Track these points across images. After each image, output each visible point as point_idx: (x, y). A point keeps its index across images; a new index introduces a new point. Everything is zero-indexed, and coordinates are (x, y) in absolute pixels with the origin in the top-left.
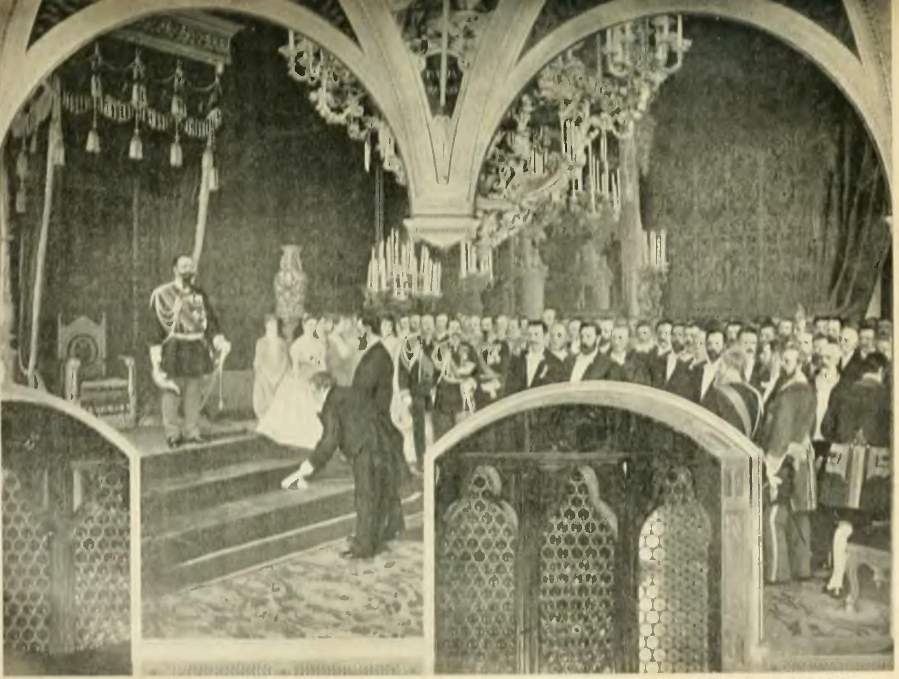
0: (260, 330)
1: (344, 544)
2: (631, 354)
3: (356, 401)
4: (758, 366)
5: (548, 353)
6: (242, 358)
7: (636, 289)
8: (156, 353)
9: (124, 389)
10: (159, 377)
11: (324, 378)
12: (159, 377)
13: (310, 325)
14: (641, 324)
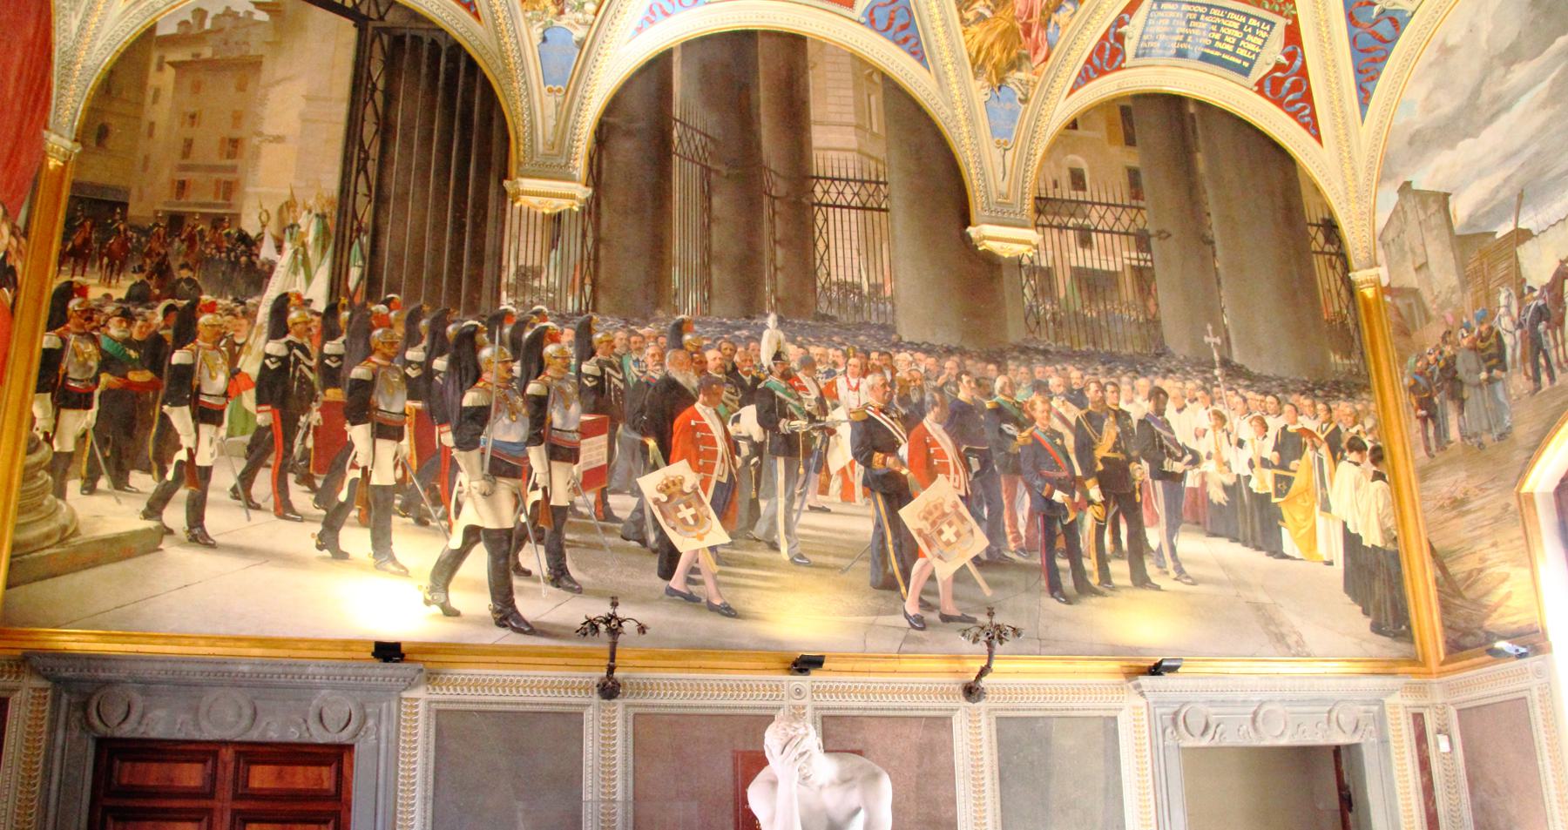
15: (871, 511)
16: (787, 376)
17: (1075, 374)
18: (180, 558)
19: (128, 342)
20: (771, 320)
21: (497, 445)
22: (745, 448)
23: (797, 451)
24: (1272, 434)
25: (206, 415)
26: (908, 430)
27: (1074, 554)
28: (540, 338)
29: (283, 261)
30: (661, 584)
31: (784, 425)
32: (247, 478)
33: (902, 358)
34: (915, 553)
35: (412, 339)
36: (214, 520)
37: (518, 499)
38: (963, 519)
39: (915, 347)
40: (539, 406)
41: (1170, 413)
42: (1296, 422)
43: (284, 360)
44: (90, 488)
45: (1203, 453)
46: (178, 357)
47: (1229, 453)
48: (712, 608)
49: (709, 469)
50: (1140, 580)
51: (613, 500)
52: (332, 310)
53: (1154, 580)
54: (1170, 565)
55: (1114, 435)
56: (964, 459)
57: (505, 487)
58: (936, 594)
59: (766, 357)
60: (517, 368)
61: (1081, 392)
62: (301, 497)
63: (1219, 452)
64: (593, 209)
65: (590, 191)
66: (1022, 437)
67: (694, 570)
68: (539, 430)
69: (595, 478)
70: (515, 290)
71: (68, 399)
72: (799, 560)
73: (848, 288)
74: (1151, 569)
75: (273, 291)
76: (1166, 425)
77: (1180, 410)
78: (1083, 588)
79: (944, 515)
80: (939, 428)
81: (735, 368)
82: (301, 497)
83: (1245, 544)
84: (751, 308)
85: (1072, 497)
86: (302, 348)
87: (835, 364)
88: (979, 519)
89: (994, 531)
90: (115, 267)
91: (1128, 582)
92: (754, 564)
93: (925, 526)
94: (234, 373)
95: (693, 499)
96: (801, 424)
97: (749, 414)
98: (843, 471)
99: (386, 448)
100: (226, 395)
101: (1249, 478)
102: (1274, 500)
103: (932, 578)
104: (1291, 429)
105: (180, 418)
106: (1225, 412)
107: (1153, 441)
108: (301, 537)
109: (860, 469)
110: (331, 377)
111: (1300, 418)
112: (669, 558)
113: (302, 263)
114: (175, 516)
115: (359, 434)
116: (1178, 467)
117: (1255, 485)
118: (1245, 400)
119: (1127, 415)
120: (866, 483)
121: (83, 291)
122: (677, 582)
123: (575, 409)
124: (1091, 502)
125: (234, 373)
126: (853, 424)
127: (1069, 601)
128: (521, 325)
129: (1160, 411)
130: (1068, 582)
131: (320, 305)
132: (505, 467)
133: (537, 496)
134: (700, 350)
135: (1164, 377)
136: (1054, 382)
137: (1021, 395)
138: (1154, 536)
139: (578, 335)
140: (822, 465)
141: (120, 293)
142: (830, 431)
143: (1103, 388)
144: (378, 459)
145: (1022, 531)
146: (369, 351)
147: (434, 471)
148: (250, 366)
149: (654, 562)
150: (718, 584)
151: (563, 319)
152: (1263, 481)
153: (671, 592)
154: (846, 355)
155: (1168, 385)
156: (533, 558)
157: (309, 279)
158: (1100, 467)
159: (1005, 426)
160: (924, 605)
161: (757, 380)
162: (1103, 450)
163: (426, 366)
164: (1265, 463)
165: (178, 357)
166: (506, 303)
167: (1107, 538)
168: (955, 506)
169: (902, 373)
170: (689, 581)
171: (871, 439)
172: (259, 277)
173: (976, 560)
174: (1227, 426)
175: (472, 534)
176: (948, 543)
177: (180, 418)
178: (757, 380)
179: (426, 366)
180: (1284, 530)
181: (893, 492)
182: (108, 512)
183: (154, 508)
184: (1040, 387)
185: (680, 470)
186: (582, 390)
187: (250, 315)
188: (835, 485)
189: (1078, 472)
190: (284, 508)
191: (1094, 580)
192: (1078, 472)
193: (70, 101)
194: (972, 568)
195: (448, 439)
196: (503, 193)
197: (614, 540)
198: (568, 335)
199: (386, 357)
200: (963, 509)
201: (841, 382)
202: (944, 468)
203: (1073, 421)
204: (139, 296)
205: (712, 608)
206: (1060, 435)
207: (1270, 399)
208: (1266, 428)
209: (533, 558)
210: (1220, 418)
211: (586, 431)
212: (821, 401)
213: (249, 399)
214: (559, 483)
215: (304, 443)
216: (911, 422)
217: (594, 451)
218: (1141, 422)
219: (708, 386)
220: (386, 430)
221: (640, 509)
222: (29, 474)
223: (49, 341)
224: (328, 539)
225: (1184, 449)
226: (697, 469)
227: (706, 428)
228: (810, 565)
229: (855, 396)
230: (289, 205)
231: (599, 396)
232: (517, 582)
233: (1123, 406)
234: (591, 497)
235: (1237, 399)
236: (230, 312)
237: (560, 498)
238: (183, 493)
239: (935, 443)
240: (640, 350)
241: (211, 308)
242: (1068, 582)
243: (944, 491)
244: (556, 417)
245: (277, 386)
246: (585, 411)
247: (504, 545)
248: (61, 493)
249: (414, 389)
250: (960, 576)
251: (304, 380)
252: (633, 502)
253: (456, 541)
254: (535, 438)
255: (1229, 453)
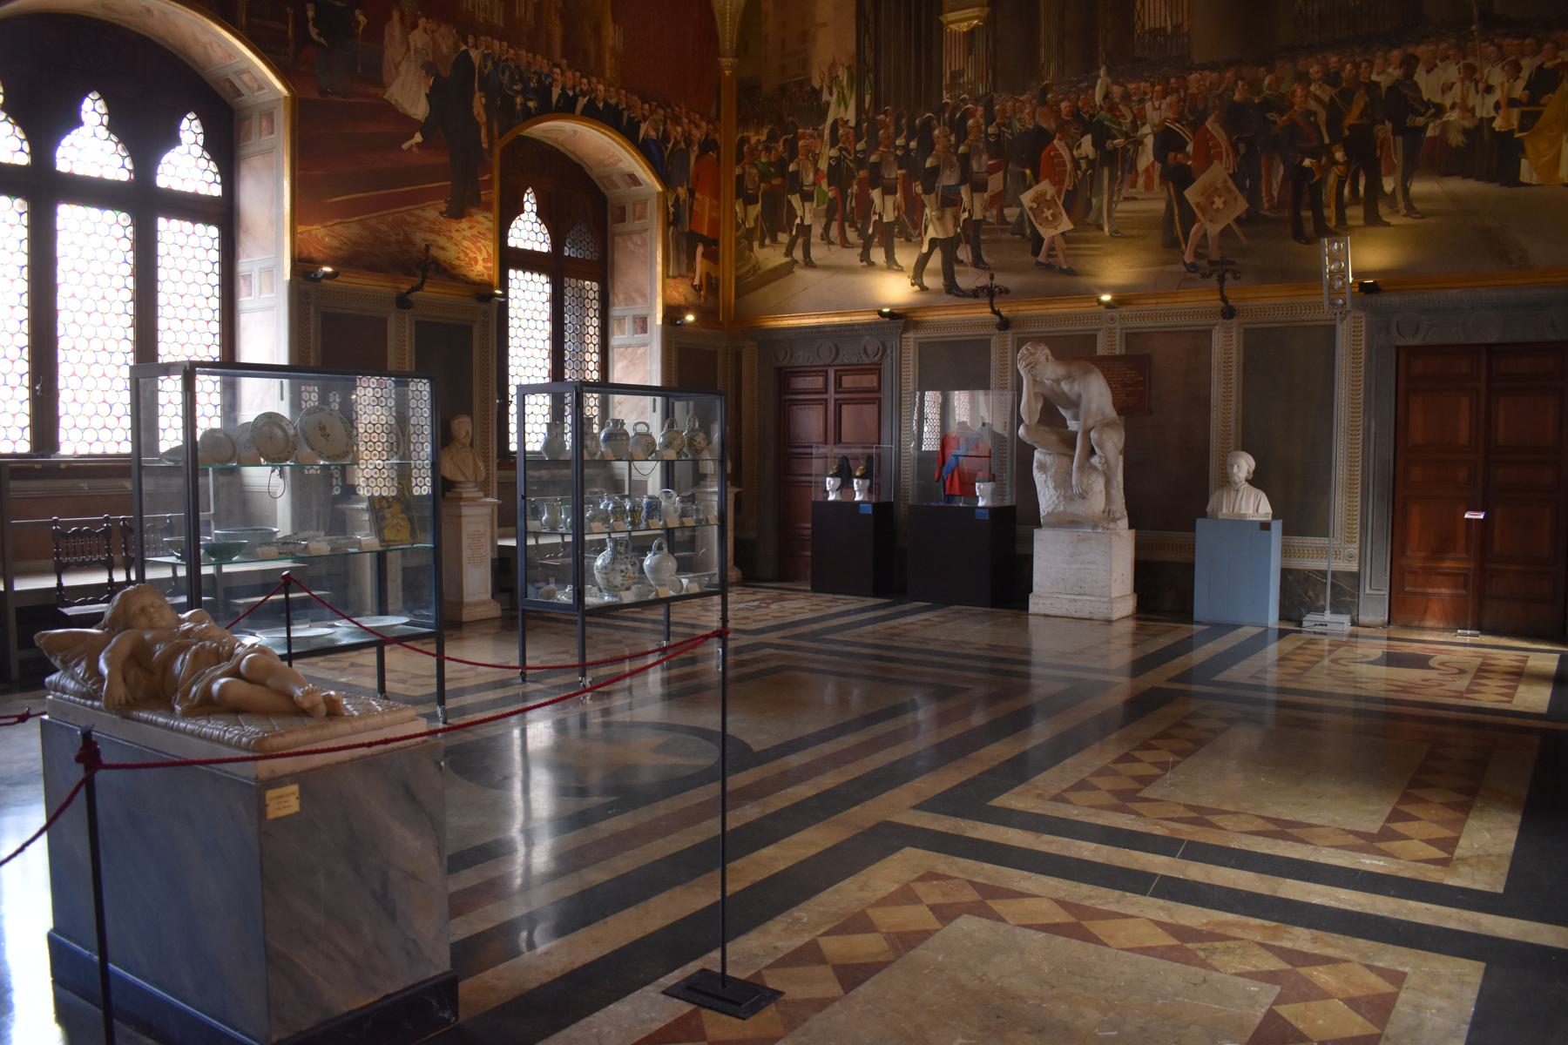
0: (390, 18)
1: (443, 207)
2: (606, 104)
3: (449, 90)
4: (665, 131)
5: (563, 89)
6: (376, 33)
7: (609, 61)
8: (310, 14)
9: (286, 33)
10: (313, 32)
11: (429, 68)
12: (313, 32)
13: (422, 22)
14: (611, 85)
15: (1165, 194)
16: (1112, 108)
17: (1333, 60)
18: (804, 275)
19: (770, 164)
20: (1102, 72)
21: (945, 188)
22: (1083, 165)
23: (1116, 161)
24: (1525, 74)
25: (807, 197)
26: (1194, 133)
27: (1317, 206)
28: (967, 114)
29: (834, 100)
30: (1031, 259)
31: (1109, 145)
32: (827, 228)
33: (1194, 76)
34: (1194, 219)
35: (897, 135)
36: (816, 253)
37: (956, 218)
38: (1229, 191)
39: (1203, 67)
40: (965, 160)
41: (1420, 77)
42: (1556, 57)
43: (838, 159)
44: (762, 245)
45: (1448, 104)
46: (792, 168)
47: (1474, 100)
48: (1063, 271)
49: (1061, 182)
50: (1373, 219)
51: (1007, 211)
52: (859, 123)
53: (1385, 219)
54: (1401, 205)
55: (1362, 104)
56: (1234, 146)
57: (949, 212)
58: (1207, 247)
59: (1098, 99)
60: (953, 138)
61: (1337, 73)
62: (852, 235)
63: (1464, 99)
64: (990, 21)
65: (987, 9)
66: (1281, 120)
67: (1052, 249)
68: (966, 177)
69: (999, 201)
70: (950, 88)
71: (750, 200)
72: (1116, 235)
73: (1155, 32)
74: (1383, 210)
75: (830, 121)
76: (1415, 87)
77: (1428, 72)
78: (1322, 230)
79: (1216, 189)
80: (1217, 126)
81: (1079, 110)
82: (852, 235)
83: (1478, 178)
84: (1089, 69)
85: (1319, 161)
86: (846, 149)
87: (1145, 93)
88: (1241, 188)
89: (1253, 196)
90: (760, 126)
91: (1361, 222)
92: (1087, 241)
93: (1201, 200)
94: (817, 171)
95: (1051, 204)
96: (1119, 141)
97: (1087, 141)
98: (1147, 170)
99: (889, 200)
100: (814, 184)
101: (1493, 119)
102: (1517, 135)
103: (1205, 236)
104: (1548, 65)
105: (795, 200)
106: (1477, 64)
107: (1402, 104)
108: (852, 257)
109: (1158, 166)
110: (861, 163)
111: (1561, 53)
112: (1037, 240)
113: (843, 100)
114: (798, 254)
115: (876, 194)
116: (1420, 121)
117: (1498, 124)
118: (1500, 47)
119: (1377, 84)
120: (1162, 176)
121: (747, 140)
122: (1041, 258)
123: (985, 157)
124: (1336, 163)
125: (817, 171)
126: (1155, 135)
127: (1309, 241)
128: (955, 109)
129: (1409, 75)
130: (1309, 228)
131: (852, 123)
132: (949, 201)
133: (966, 215)
134: (1057, 103)
135: (1418, 44)
136: (1314, 70)
137: (1284, 88)
138: (1388, 185)
139: (985, 110)
140: (1133, 167)
141: (763, 138)
142: (1139, 143)
143: (1357, 66)
144: (886, 207)
145: (1275, 194)
146: (878, 144)
147: (912, 209)
148: (823, 165)
149: (1029, 247)
150: (1066, 256)
151: (976, 101)
152: (1507, 119)
153: (1038, 263)
154: (1153, 85)
155: (1422, 50)
156: (964, 253)
157: (846, 108)
158: (1347, 133)
159: (1268, 115)
160: (1197, 255)
161: (1092, 116)
162: (1352, 118)
163: (906, 147)
164: (1513, 103)
165: (792, 168)
166: (946, 100)
167: (1346, 191)
168: (1226, 182)
169: (1192, 90)
170: (1049, 256)
171: (1167, 142)
172: (823, 111)
173: (1238, 220)
174: (1477, 76)
175: (933, 243)
176: (1218, 210)
177: (795, 200)
178: (1092, 116)
179: (906, 147)
180: (1524, 162)
181: (1179, 178)
182: (771, 256)
183: (789, 253)
184: (1303, 78)
185: (1045, 186)
186: (988, 142)
187: (821, 136)
188: (1141, 181)
189: (1327, 140)
190: (845, 243)
191: (1332, 224)
192: (1327, 140)
193: (728, 34)
194: (1235, 227)
195: (919, 189)
196: (941, 26)
197: (1007, 236)
198: (980, 110)
199: (888, 146)
200: (1230, 183)
201: (1148, 105)
202: (1219, 156)
203: (1326, 99)
204: (772, 137)
205: (1063, 271)
206: (1315, 114)
207: (1528, 41)
208: (1519, 69)
209: (964, 253)
210: (1470, 72)
211: (992, 170)
212: (1134, 122)
213: (824, 185)
214: (974, 205)
215: (851, 203)
216: (1197, 125)
217: (995, 182)
218: (1389, 88)
219: (1062, 127)
220: (888, 190)
221: (1021, 215)
222: (738, 243)
223: (738, 171)
224: (865, 256)
225: (1428, 105)
226: (1054, 183)
227: (1060, 156)
228: (1123, 237)
229: (1158, 112)
230: (833, 65)
231: (997, 148)
232: (956, 268)
233: (1374, 77)
234: (994, 212)
235: (1492, 48)
236: (812, 136)
237: (977, 215)
238: (800, 241)
239: (1213, 138)
240: (1022, 111)
241: (803, 136)
242: (1309, 228)
243: (1218, 172)
244: (975, 166)
245: (838, 175)
246: (991, 158)
247: (947, 247)
248: (751, 250)
249: (902, 162)
250: (1226, 232)
251: (849, 168)
252: (1018, 210)
253: (925, 249)
254: (963, 181)
255: (1474, 100)
